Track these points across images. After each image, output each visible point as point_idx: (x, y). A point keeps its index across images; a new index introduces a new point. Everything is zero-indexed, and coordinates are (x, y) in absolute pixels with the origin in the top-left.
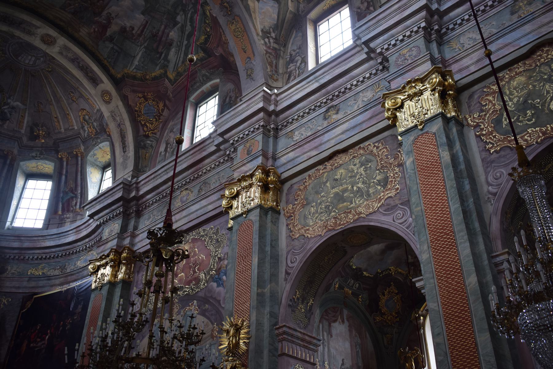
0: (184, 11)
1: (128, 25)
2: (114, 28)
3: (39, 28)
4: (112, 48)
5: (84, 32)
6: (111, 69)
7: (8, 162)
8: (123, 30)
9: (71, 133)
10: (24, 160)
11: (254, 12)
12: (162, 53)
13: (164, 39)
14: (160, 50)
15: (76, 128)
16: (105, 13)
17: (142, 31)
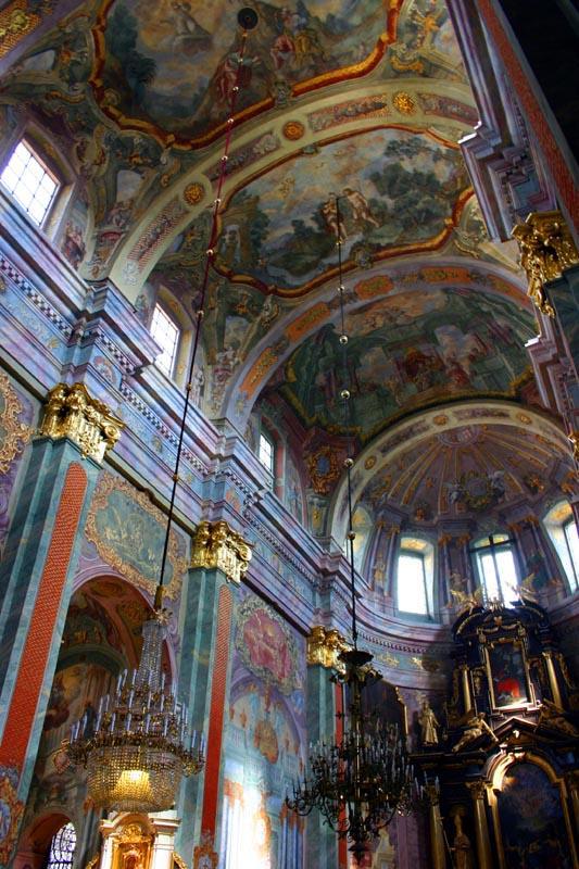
0: (477, 301)
1: (469, 351)
2: (466, 366)
3: (424, 421)
4: (484, 378)
5: (454, 389)
6: (502, 394)
7: (534, 528)
8: (472, 358)
9: (552, 463)
10: (544, 517)
11: (497, 254)
12: (515, 343)
13: (502, 333)
14: (511, 342)
15: (550, 455)
16: (445, 361)
17: (483, 344)
